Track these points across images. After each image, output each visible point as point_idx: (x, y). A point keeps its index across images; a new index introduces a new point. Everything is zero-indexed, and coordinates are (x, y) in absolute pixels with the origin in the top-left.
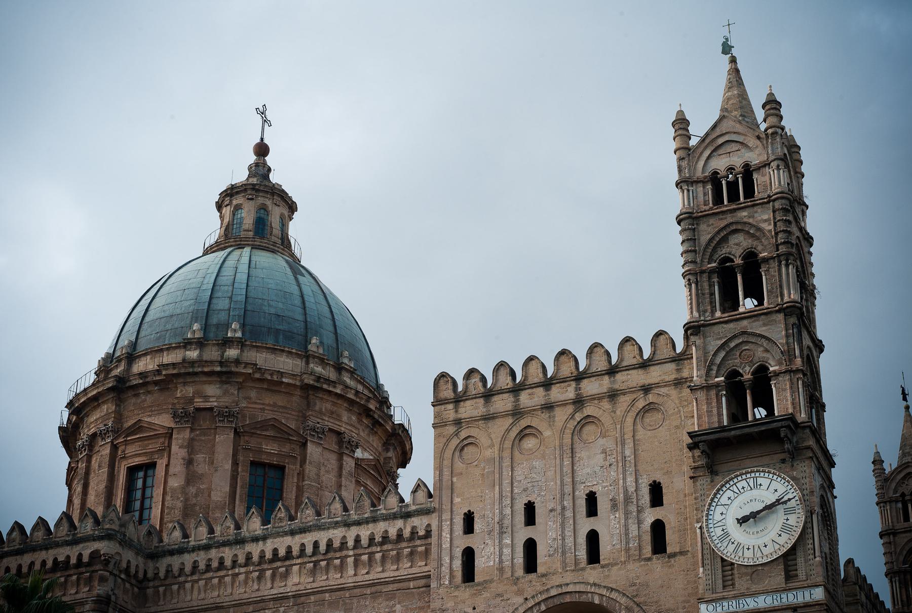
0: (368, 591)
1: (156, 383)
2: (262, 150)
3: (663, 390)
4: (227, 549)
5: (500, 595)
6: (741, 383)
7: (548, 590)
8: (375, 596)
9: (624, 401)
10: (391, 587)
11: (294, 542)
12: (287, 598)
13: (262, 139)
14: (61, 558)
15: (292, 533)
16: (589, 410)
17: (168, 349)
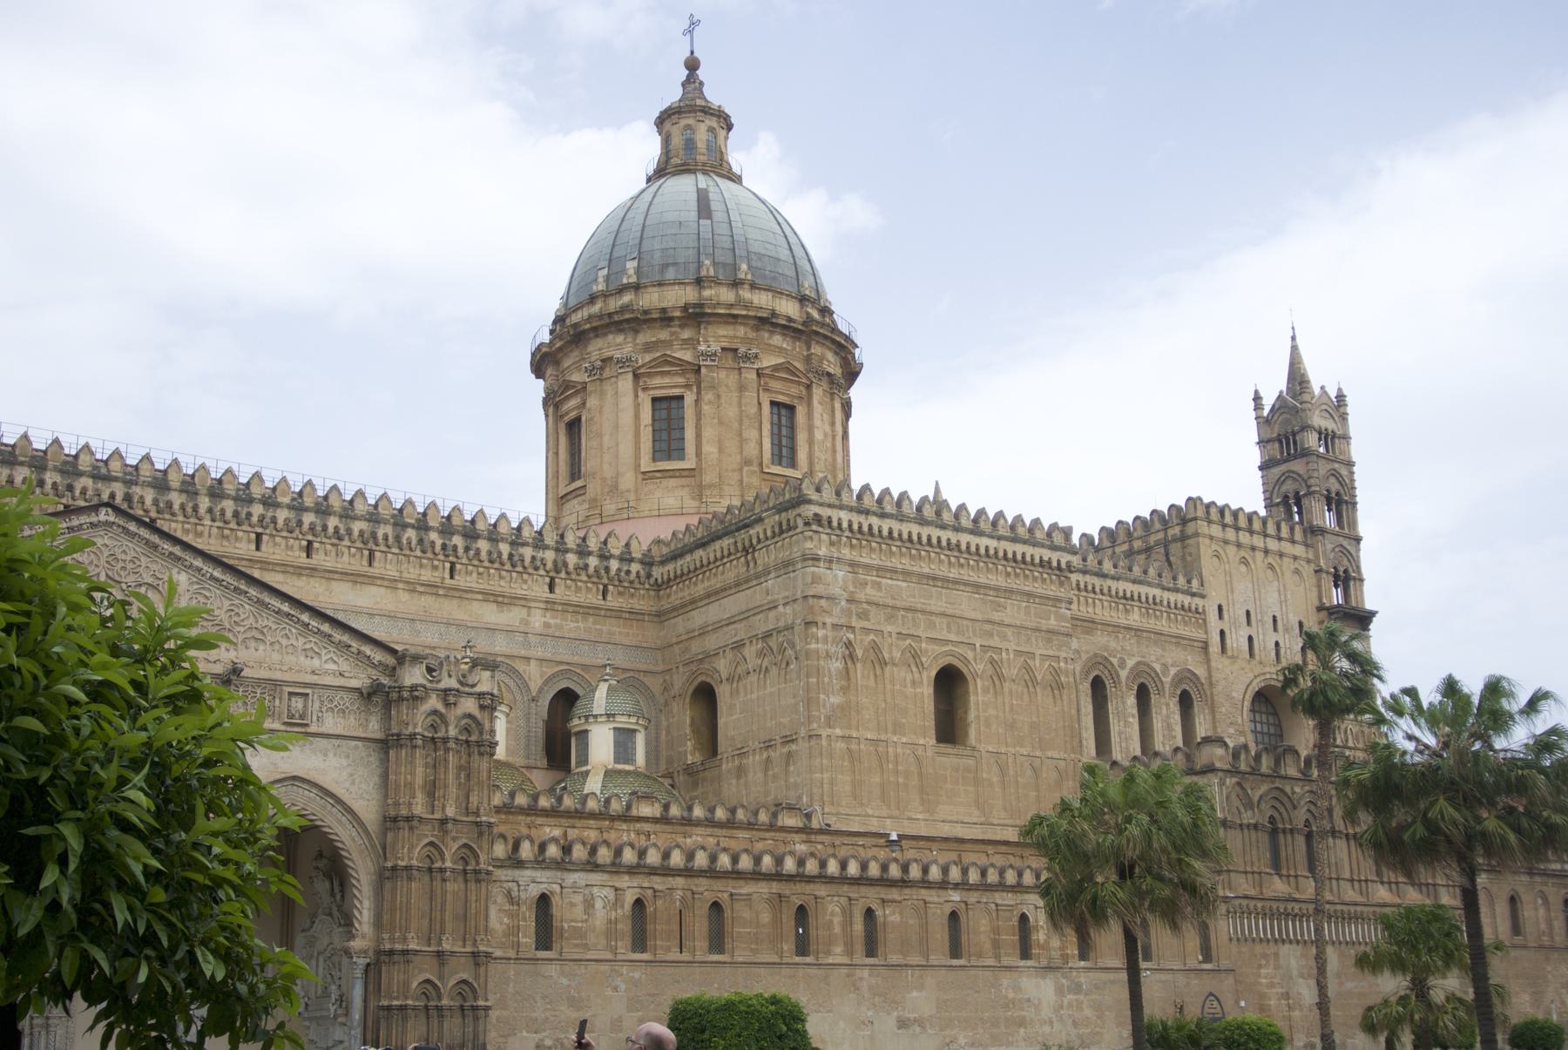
0: (1174, 640)
1: (796, 330)
2: (692, 65)
3: (1302, 563)
4: (1096, 578)
5: (1243, 669)
6: (1339, 576)
7: (1264, 674)
8: (1177, 644)
9: (1286, 560)
10: (1185, 642)
11: (1136, 589)
12: (1132, 629)
13: (692, 53)
14: (1046, 558)
15: (1134, 582)
16: (1270, 559)
17: (787, 295)
